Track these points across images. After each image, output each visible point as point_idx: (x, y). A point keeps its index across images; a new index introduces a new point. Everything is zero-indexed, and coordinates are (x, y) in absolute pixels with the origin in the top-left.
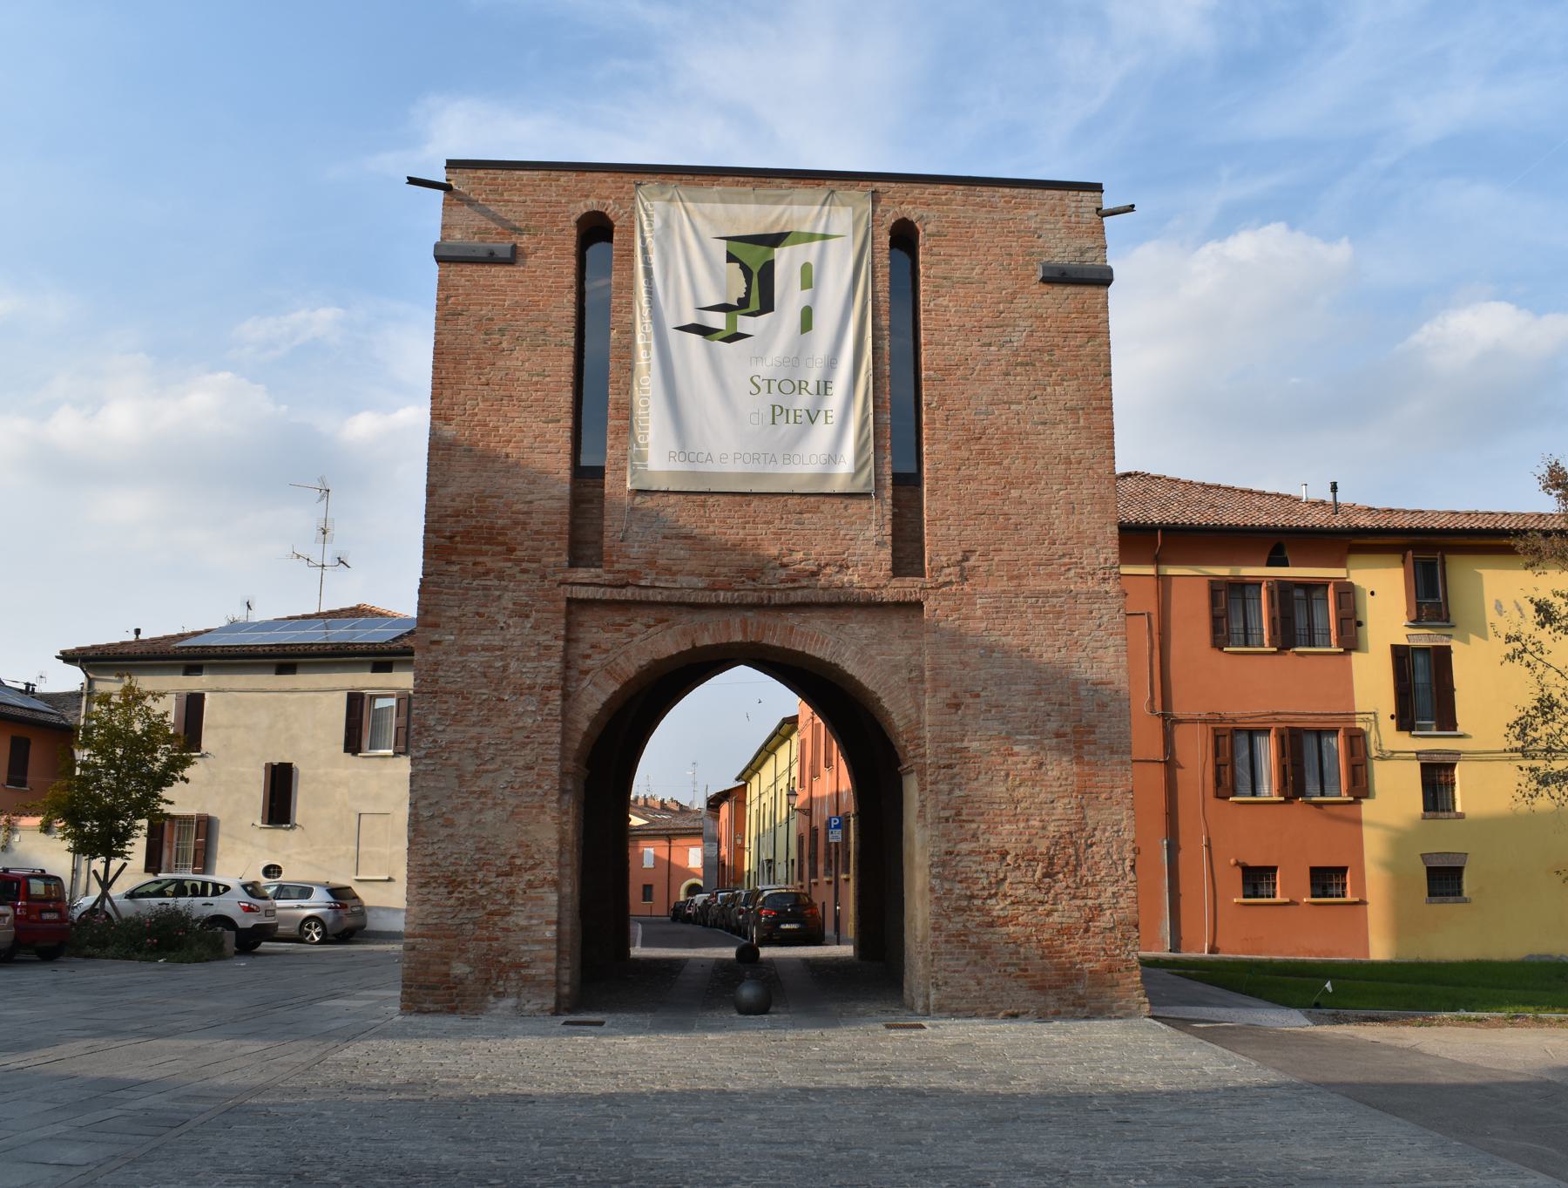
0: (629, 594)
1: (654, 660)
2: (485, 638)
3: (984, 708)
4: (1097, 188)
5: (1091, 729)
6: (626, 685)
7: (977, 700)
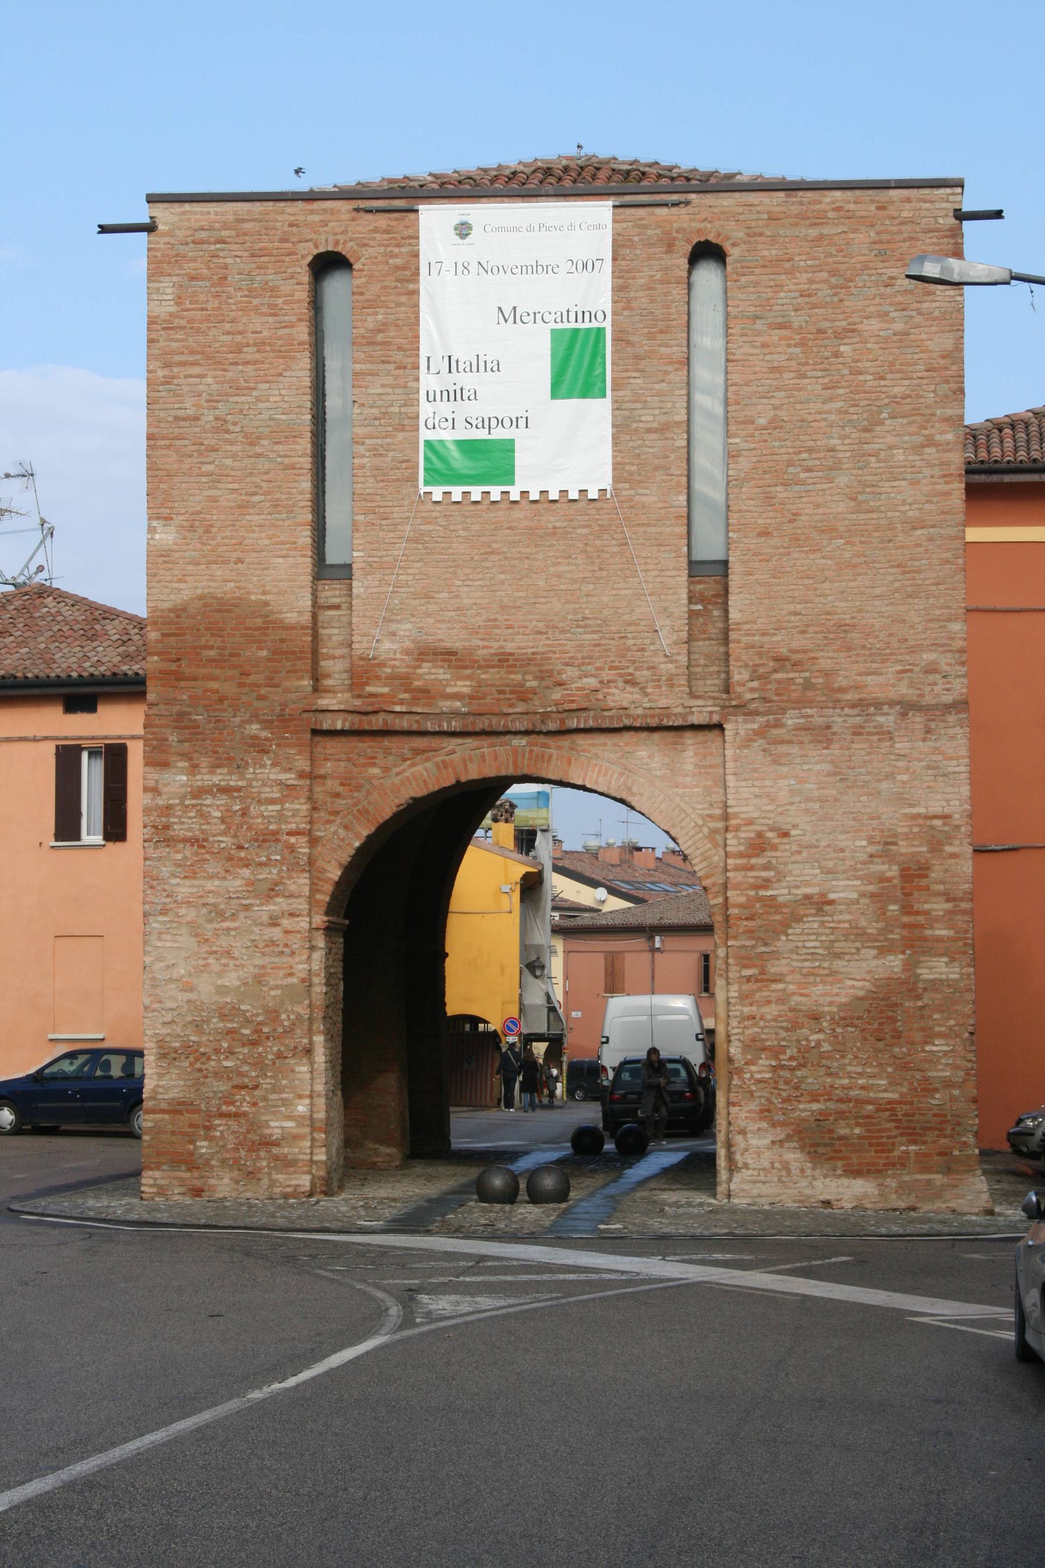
0: (381, 722)
1: (414, 799)
2: (220, 777)
3: (794, 848)
4: (960, 184)
5: (923, 870)
6: (382, 828)
7: (785, 840)
